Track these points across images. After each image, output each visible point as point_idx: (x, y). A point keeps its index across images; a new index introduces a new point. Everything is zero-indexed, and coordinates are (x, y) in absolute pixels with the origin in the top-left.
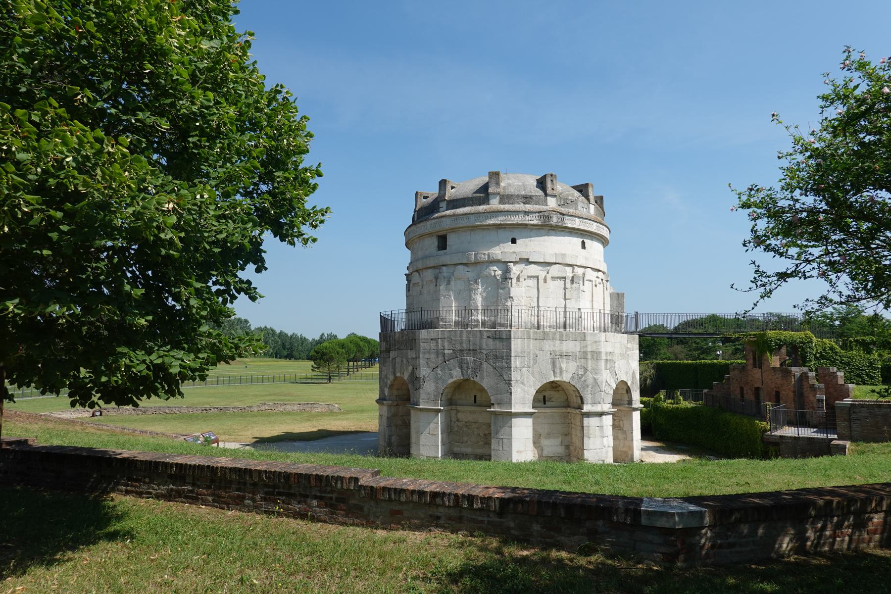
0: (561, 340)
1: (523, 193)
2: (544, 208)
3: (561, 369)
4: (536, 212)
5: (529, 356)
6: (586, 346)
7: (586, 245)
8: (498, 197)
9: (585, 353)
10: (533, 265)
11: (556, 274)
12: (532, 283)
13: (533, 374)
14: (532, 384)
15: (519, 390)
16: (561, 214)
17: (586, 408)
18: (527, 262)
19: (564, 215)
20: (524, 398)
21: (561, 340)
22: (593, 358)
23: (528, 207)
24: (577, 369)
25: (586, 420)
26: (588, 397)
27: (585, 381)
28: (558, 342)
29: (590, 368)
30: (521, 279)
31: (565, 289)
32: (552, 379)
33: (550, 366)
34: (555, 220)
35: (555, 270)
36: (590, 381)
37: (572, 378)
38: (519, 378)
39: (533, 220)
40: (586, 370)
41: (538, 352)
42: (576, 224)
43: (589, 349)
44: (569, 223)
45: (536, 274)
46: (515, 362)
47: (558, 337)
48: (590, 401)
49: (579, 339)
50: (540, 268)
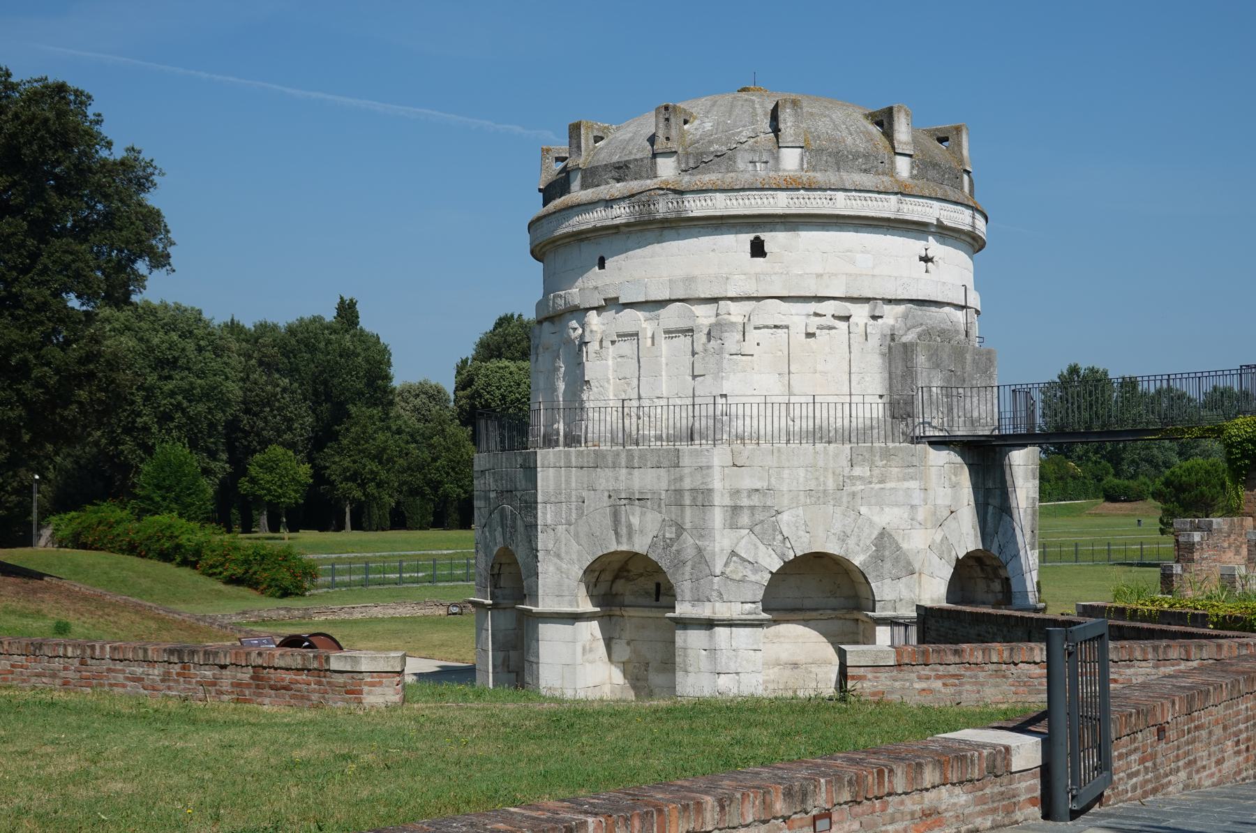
0: (630, 467)
1: (615, 159)
2: (650, 183)
3: (630, 526)
4: (623, 199)
5: (568, 502)
6: (681, 479)
7: (766, 249)
8: (579, 176)
9: (679, 492)
10: (628, 311)
11: (672, 326)
12: (627, 347)
13: (577, 536)
14: (574, 557)
15: (551, 569)
16: (675, 191)
17: (683, 609)
18: (613, 304)
19: (681, 193)
20: (560, 585)
21: (630, 467)
22: (694, 504)
23: (617, 189)
24: (662, 528)
25: (680, 636)
26: (684, 587)
27: (678, 552)
28: (624, 471)
29: (688, 525)
30: (607, 343)
31: (694, 353)
32: (613, 547)
33: (608, 521)
34: (663, 208)
35: (672, 316)
36: (690, 553)
37: (653, 545)
38: (550, 546)
39: (621, 214)
40: (680, 529)
41: (584, 494)
42: (720, 205)
43: (687, 484)
44: (697, 207)
45: (633, 330)
46: (545, 515)
47: (623, 464)
48: (688, 595)
49: (666, 463)
50: (640, 315)
